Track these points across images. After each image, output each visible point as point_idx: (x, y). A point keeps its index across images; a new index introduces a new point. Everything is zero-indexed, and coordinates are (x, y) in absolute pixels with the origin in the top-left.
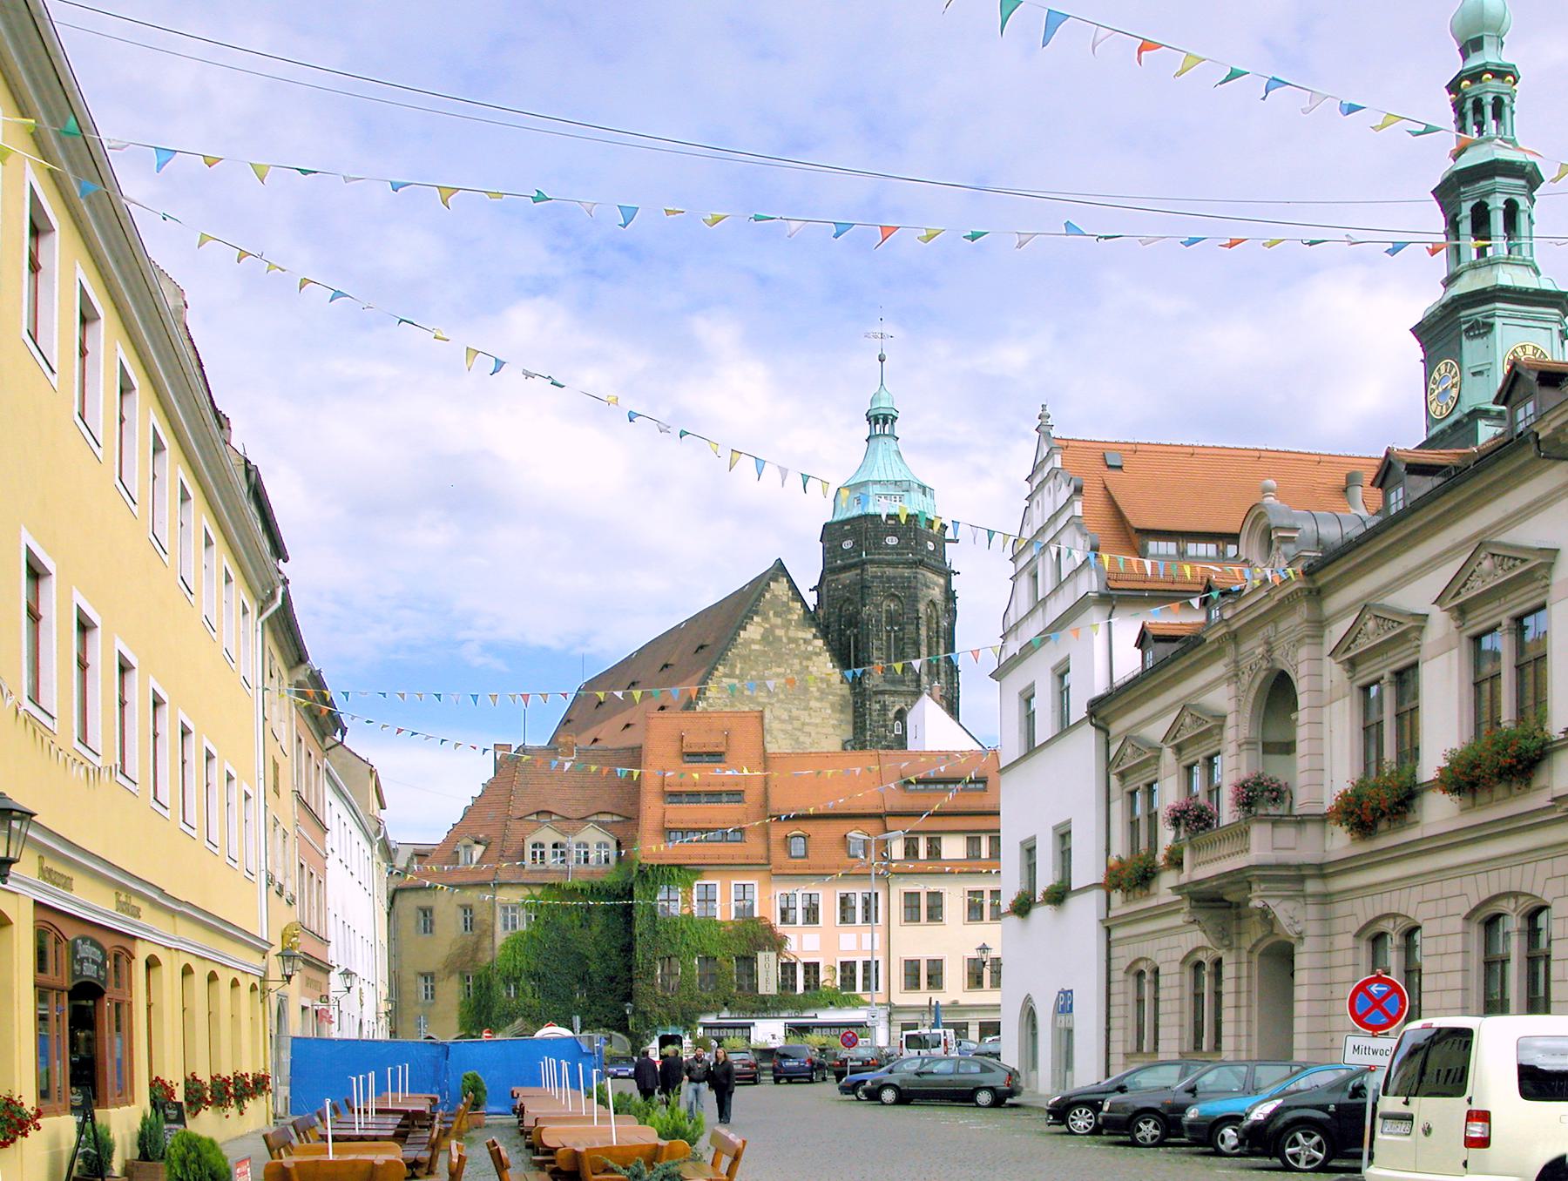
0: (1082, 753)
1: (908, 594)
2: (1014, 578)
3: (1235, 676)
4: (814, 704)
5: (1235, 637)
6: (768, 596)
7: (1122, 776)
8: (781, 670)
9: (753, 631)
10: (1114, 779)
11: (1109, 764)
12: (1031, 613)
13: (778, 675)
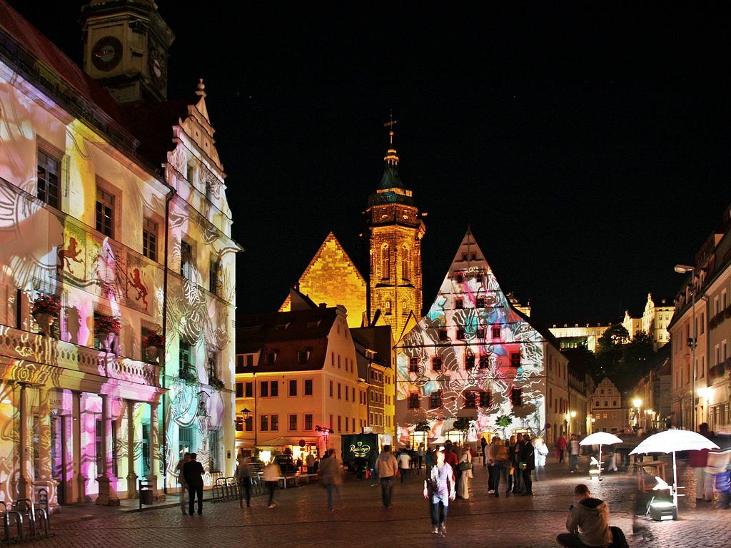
8: (332, 282)
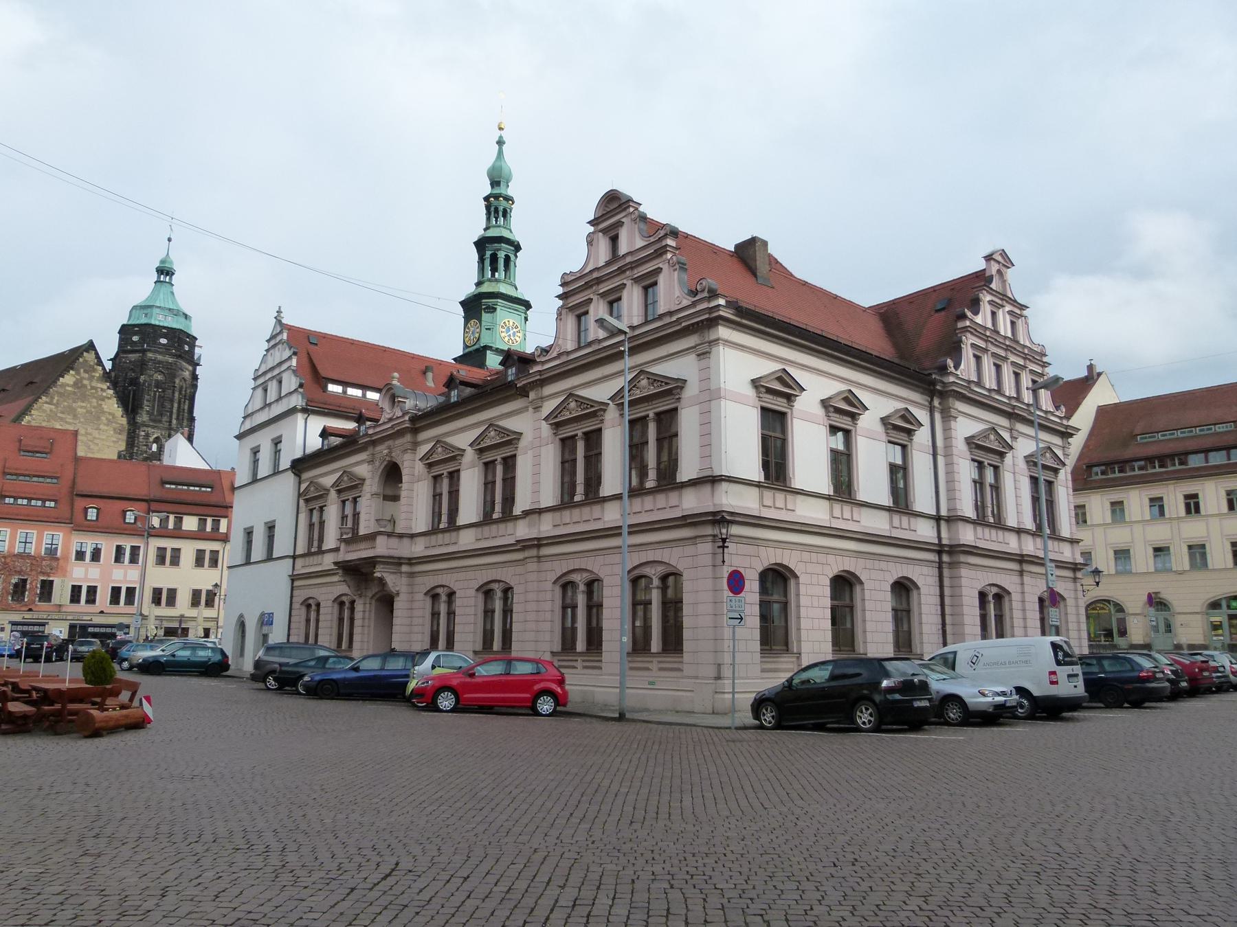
0: (286, 485)
1: (171, 372)
2: (254, 389)
3: (371, 462)
4: (102, 427)
5: (374, 443)
7: (307, 501)
9: (69, 379)
10: (302, 502)
11: (300, 495)
12: (262, 409)
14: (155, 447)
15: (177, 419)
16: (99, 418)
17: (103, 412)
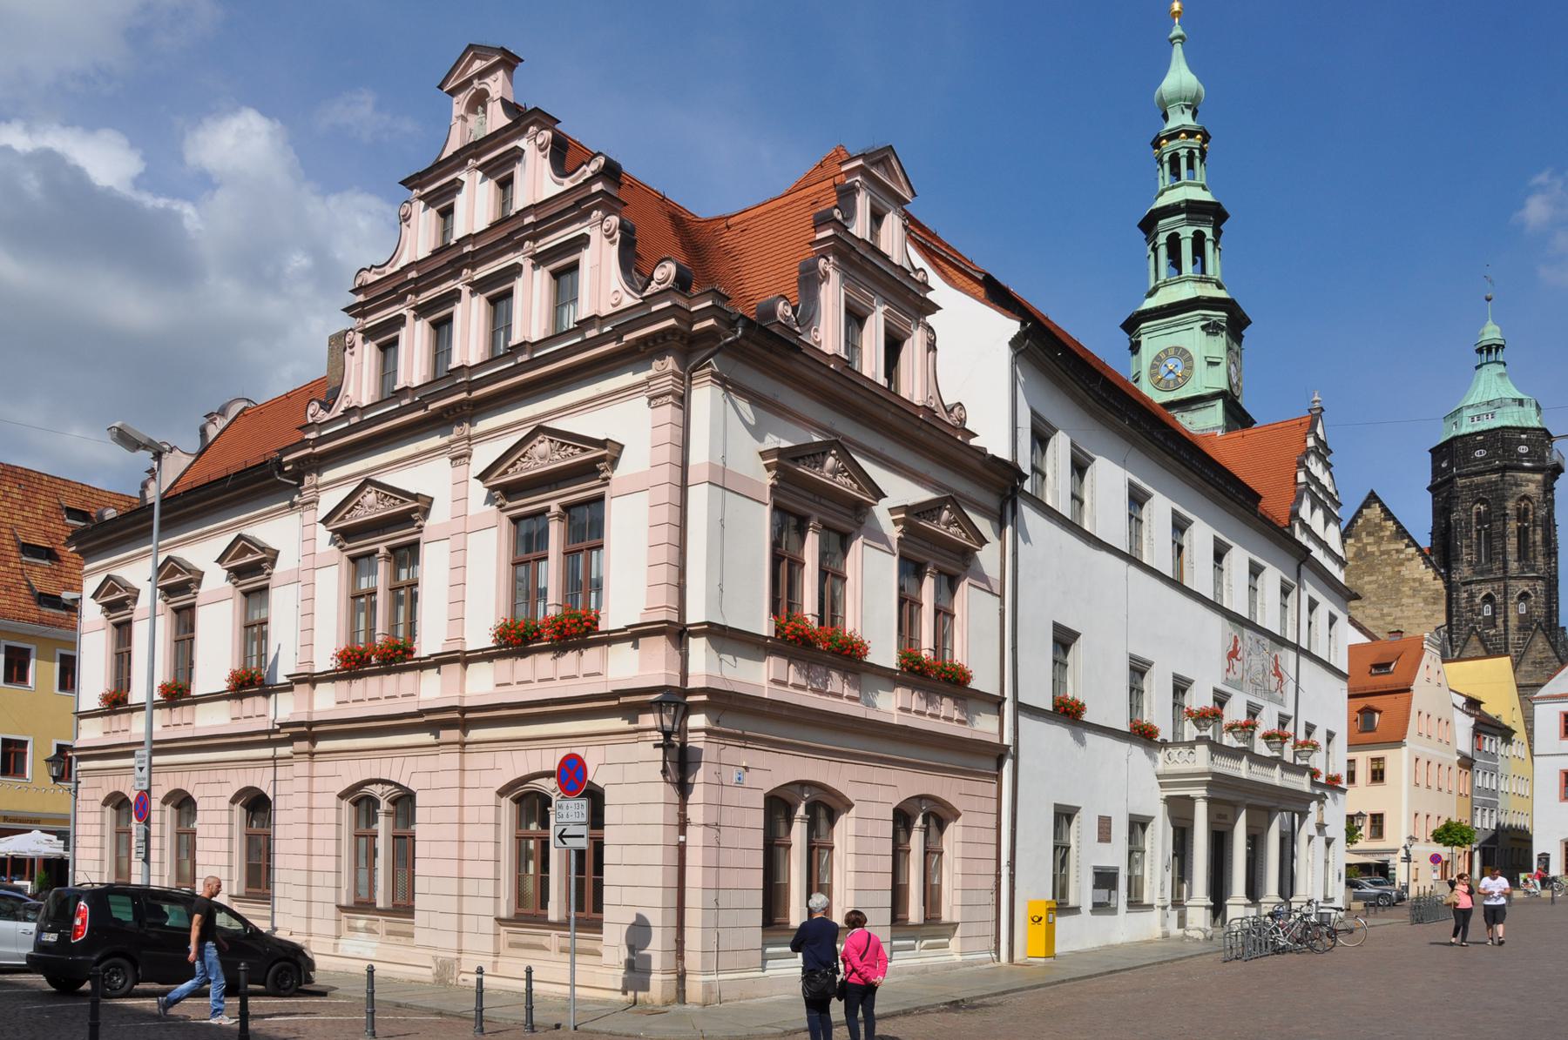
4: (1404, 601)
6: (1360, 521)
13: (1370, 583)
14: (1487, 610)
15: (1519, 560)
16: (1398, 591)
17: (1404, 581)
